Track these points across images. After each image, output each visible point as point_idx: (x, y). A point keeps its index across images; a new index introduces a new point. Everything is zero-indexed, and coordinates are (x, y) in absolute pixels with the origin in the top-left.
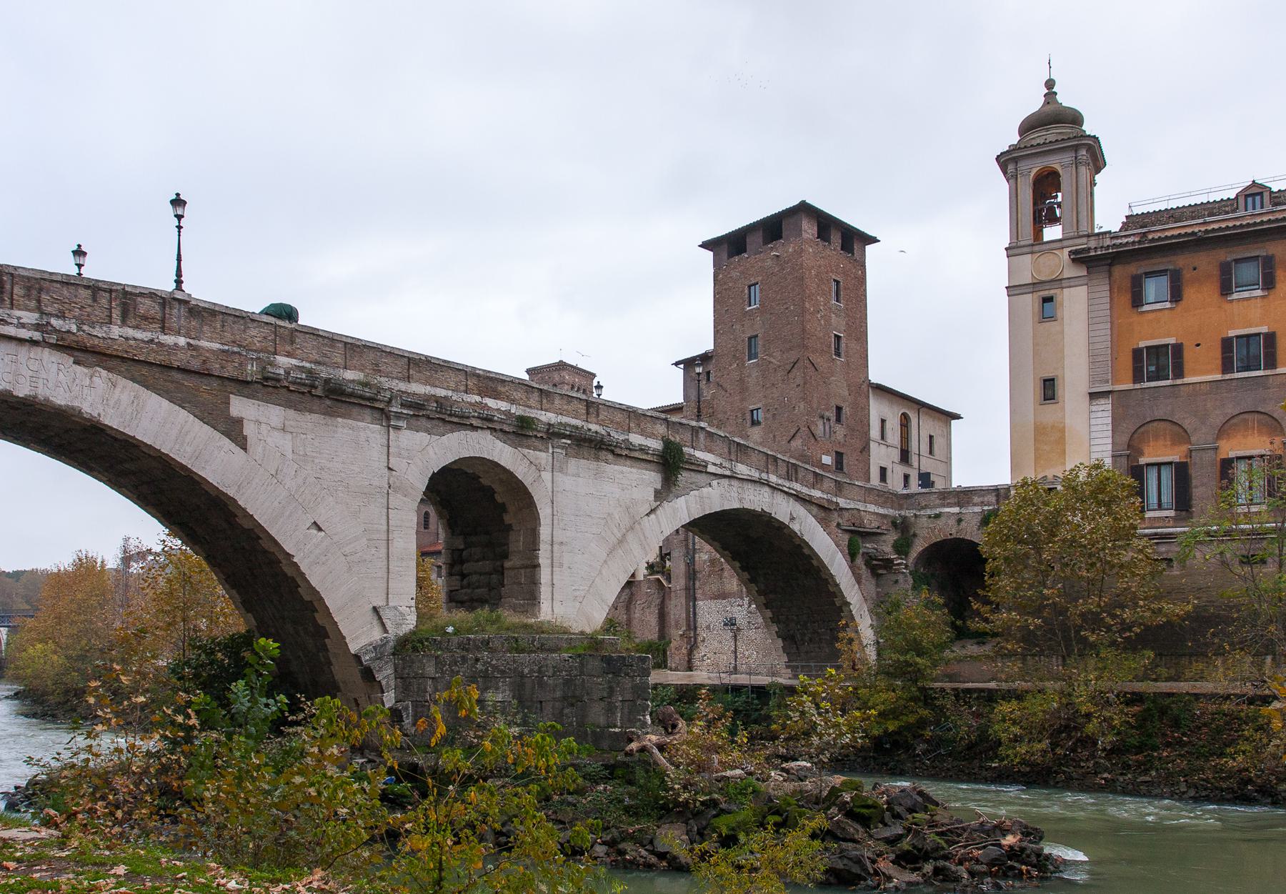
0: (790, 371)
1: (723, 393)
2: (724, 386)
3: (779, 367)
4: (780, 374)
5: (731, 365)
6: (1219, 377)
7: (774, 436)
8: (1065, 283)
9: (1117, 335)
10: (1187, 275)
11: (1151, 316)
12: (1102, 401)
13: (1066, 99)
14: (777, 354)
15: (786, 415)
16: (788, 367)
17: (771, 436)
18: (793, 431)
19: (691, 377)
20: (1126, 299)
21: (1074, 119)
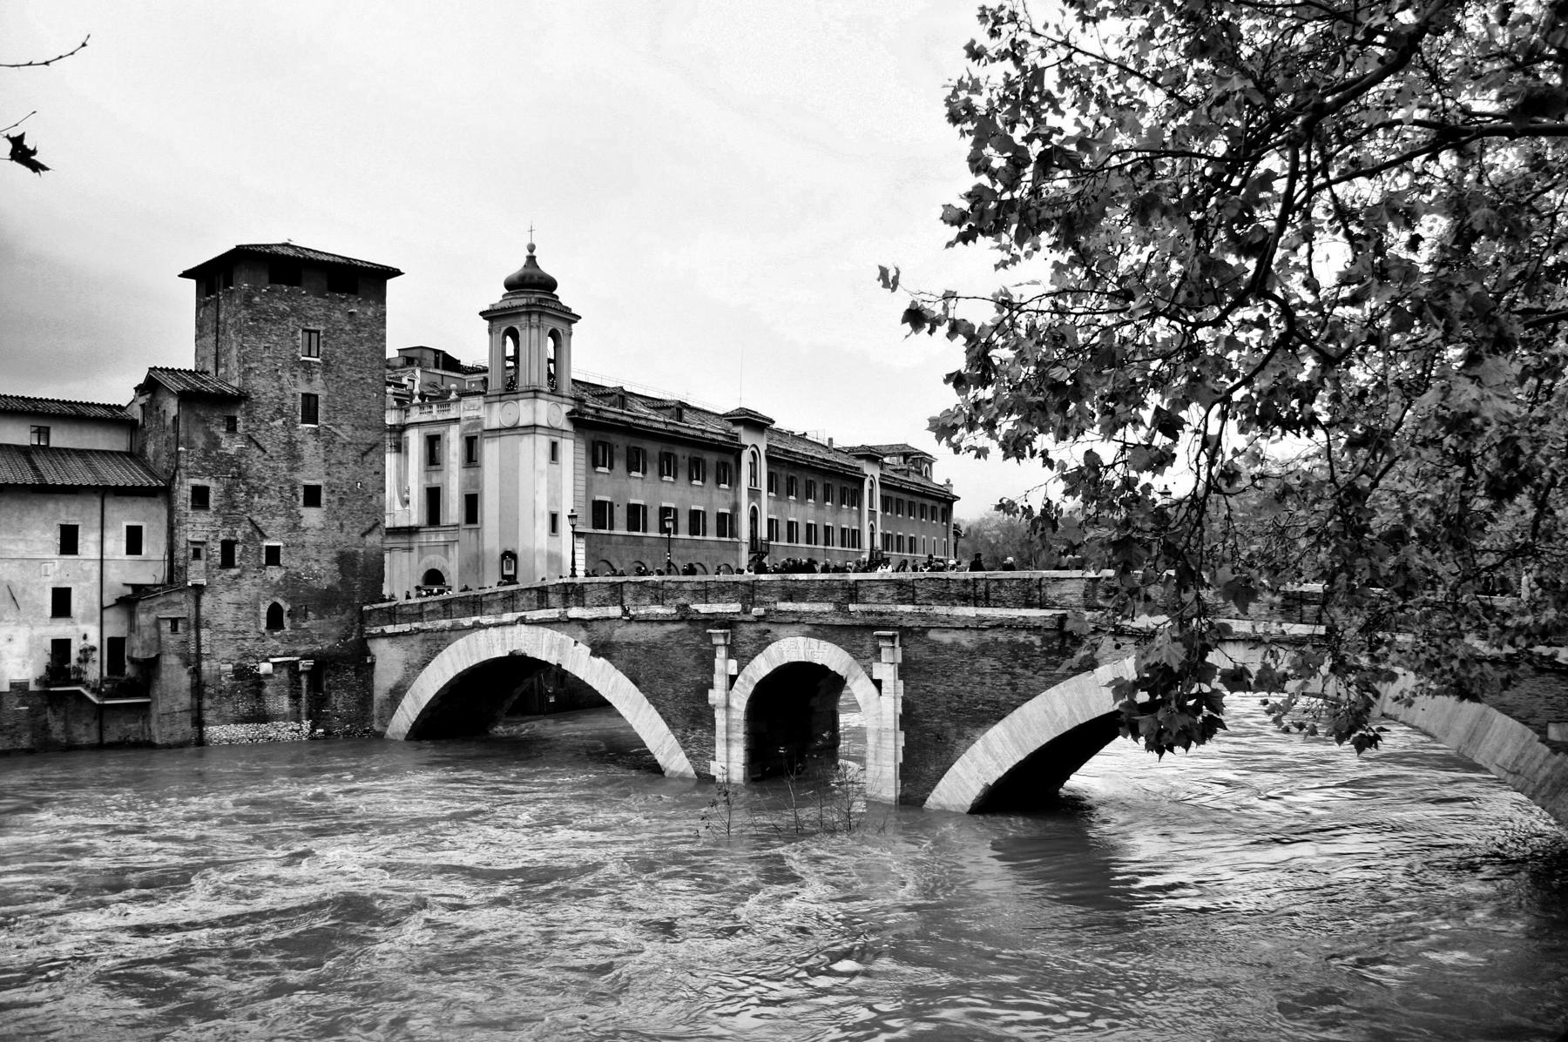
0: (365, 454)
1: (259, 452)
2: (261, 442)
3: (350, 444)
4: (351, 454)
5: (273, 420)
6: (626, 533)
7: (342, 525)
8: (564, 434)
9: (589, 486)
10: (615, 450)
11: (600, 476)
12: (582, 540)
13: (547, 266)
14: (348, 429)
15: (359, 503)
16: (363, 448)
17: (337, 523)
18: (368, 524)
19: (198, 415)
20: (590, 462)
21: (549, 285)
